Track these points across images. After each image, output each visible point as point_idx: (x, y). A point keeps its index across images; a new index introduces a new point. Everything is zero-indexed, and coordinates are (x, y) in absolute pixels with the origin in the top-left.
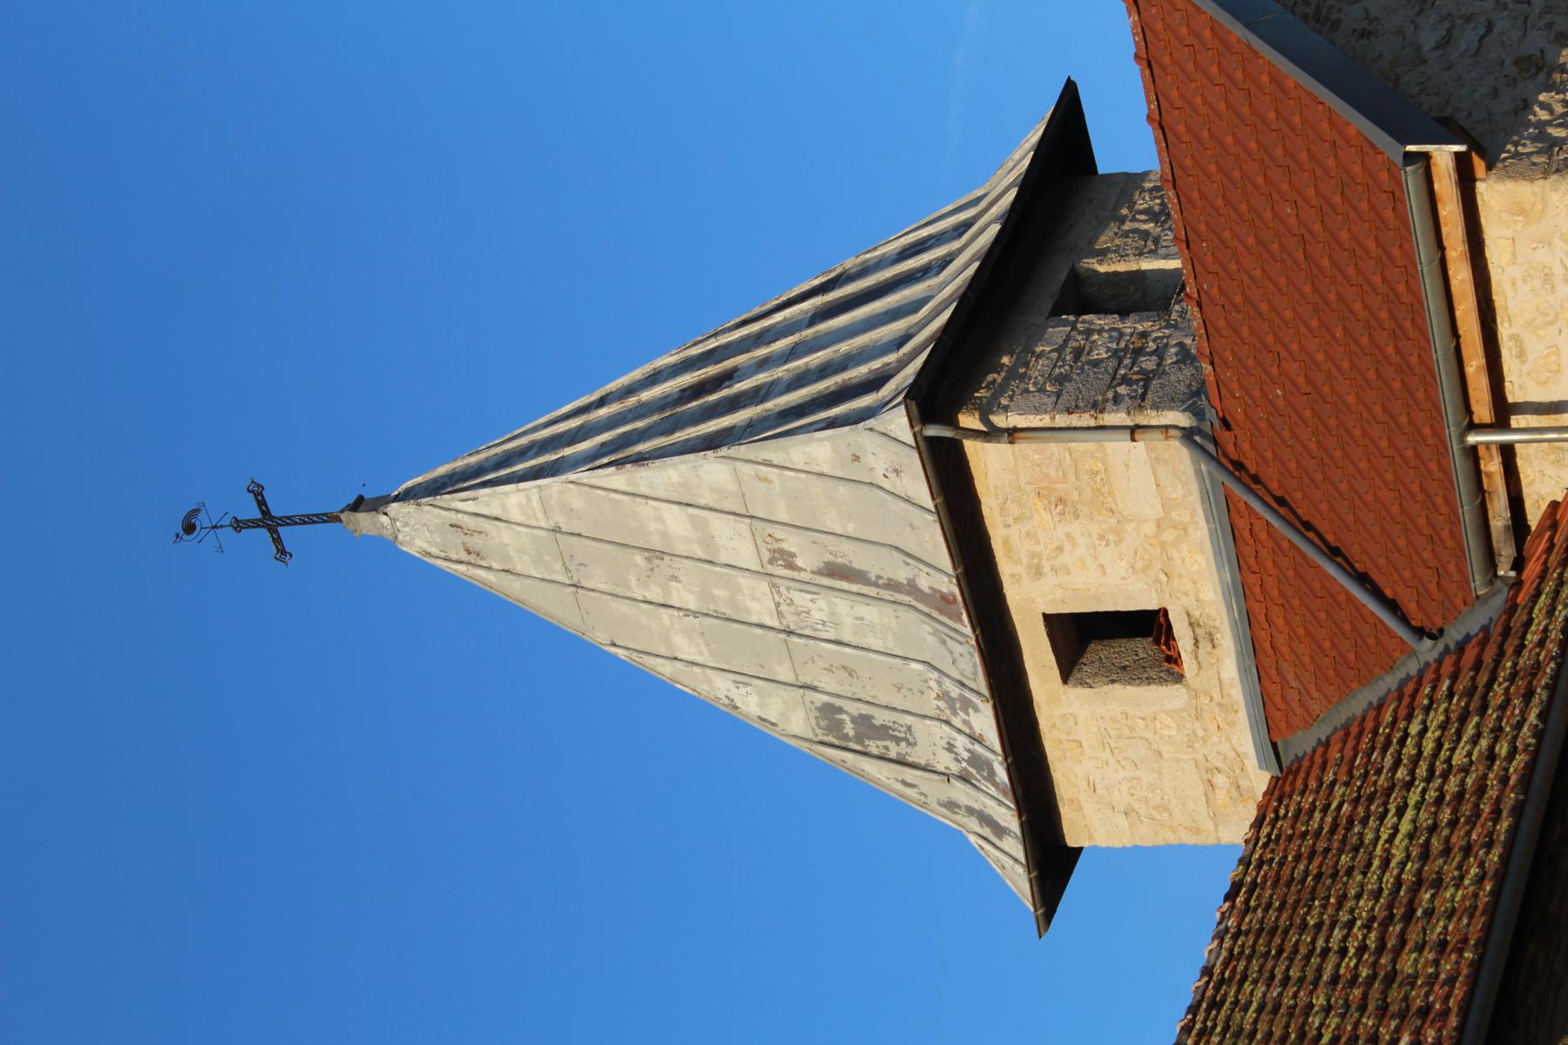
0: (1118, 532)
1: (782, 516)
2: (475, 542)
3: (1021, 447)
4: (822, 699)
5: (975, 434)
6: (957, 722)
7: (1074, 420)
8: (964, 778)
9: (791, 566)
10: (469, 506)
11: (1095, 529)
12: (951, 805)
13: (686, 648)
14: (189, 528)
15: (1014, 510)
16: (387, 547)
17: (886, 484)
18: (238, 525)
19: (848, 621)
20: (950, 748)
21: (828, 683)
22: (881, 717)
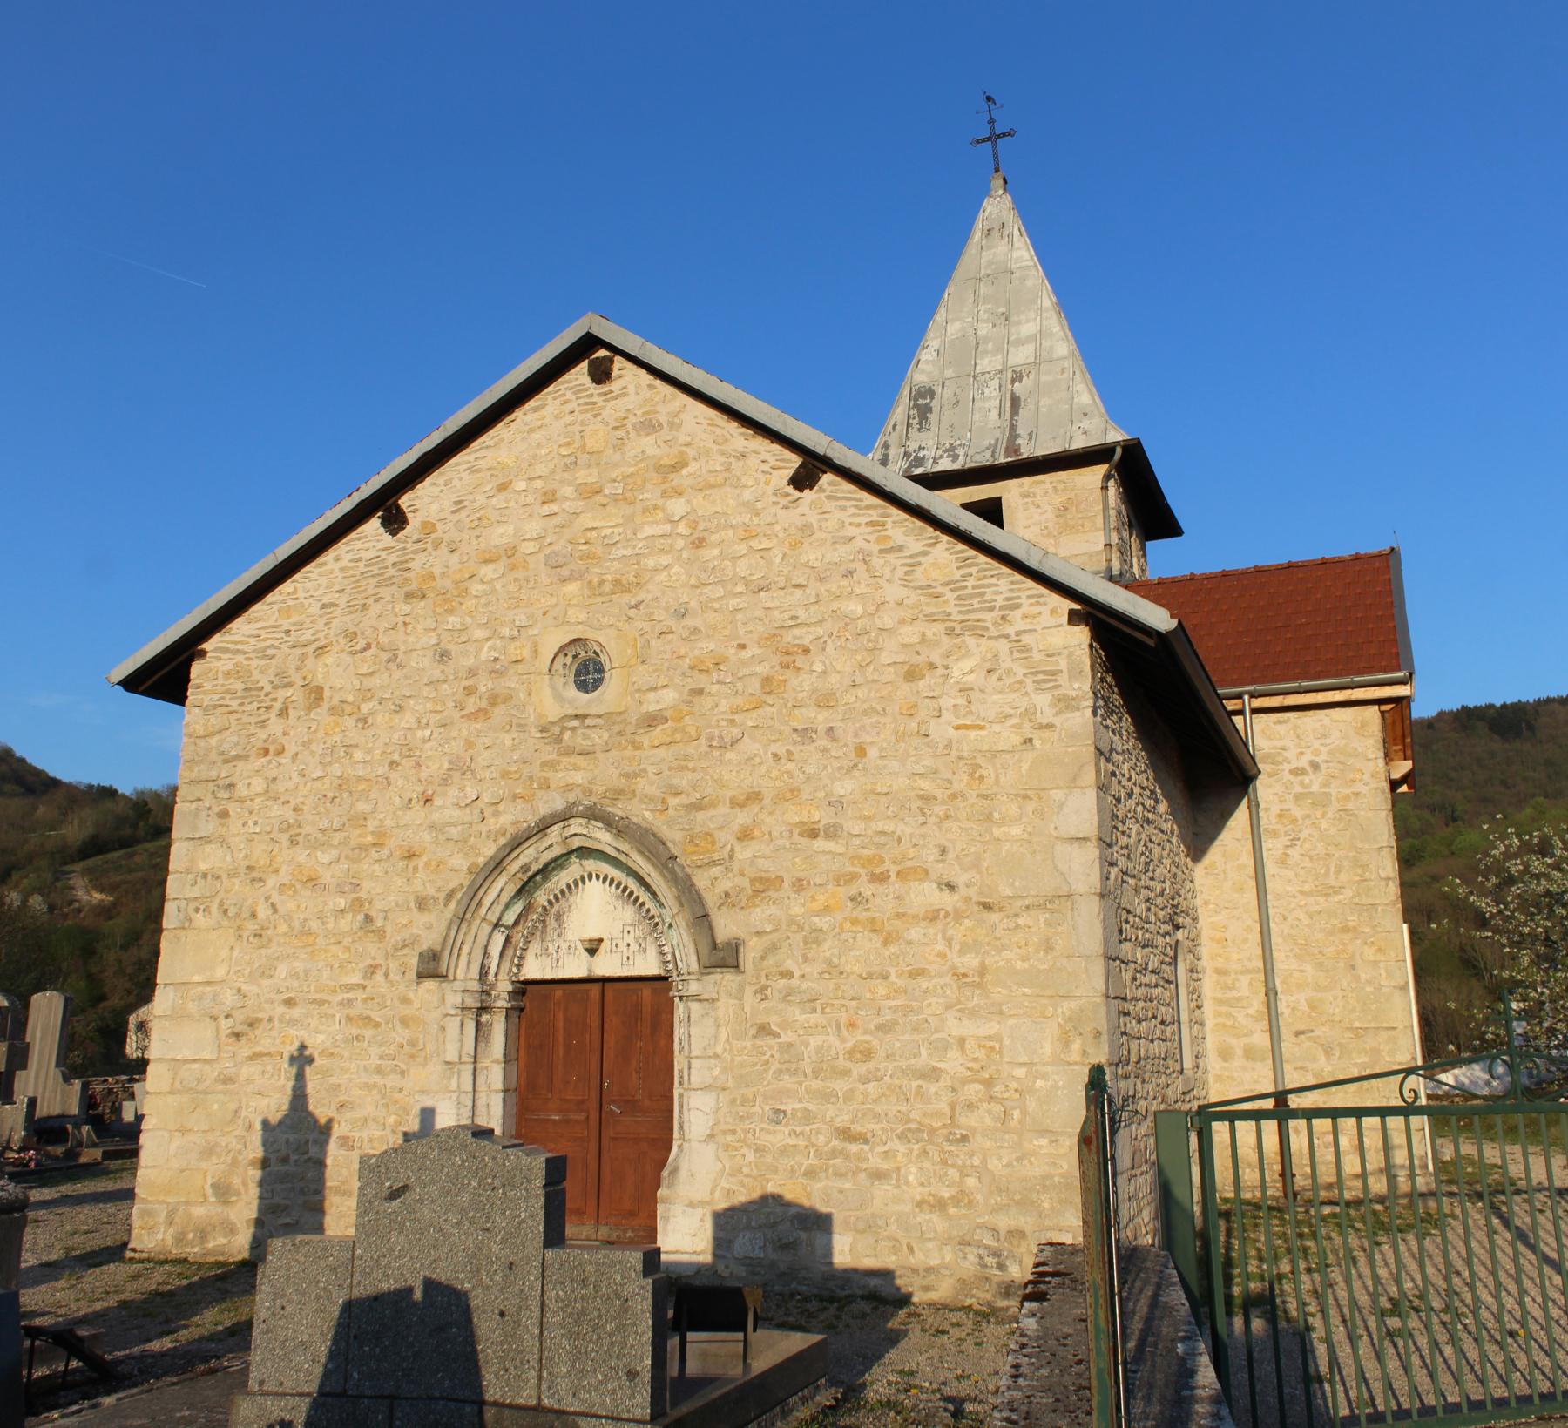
0: (1049, 535)
1: (1043, 378)
2: (996, 234)
3: (1099, 492)
4: (938, 390)
5: (1109, 471)
6: (940, 452)
7: (1113, 519)
8: (907, 454)
9: (1013, 381)
10: (1016, 232)
11: (1050, 525)
12: (886, 446)
13: (954, 328)
14: (989, 99)
15: (1060, 487)
16: (986, 192)
17: (1075, 428)
18: (992, 122)
19: (987, 405)
20: (921, 448)
21: (948, 393)
22: (932, 417)
